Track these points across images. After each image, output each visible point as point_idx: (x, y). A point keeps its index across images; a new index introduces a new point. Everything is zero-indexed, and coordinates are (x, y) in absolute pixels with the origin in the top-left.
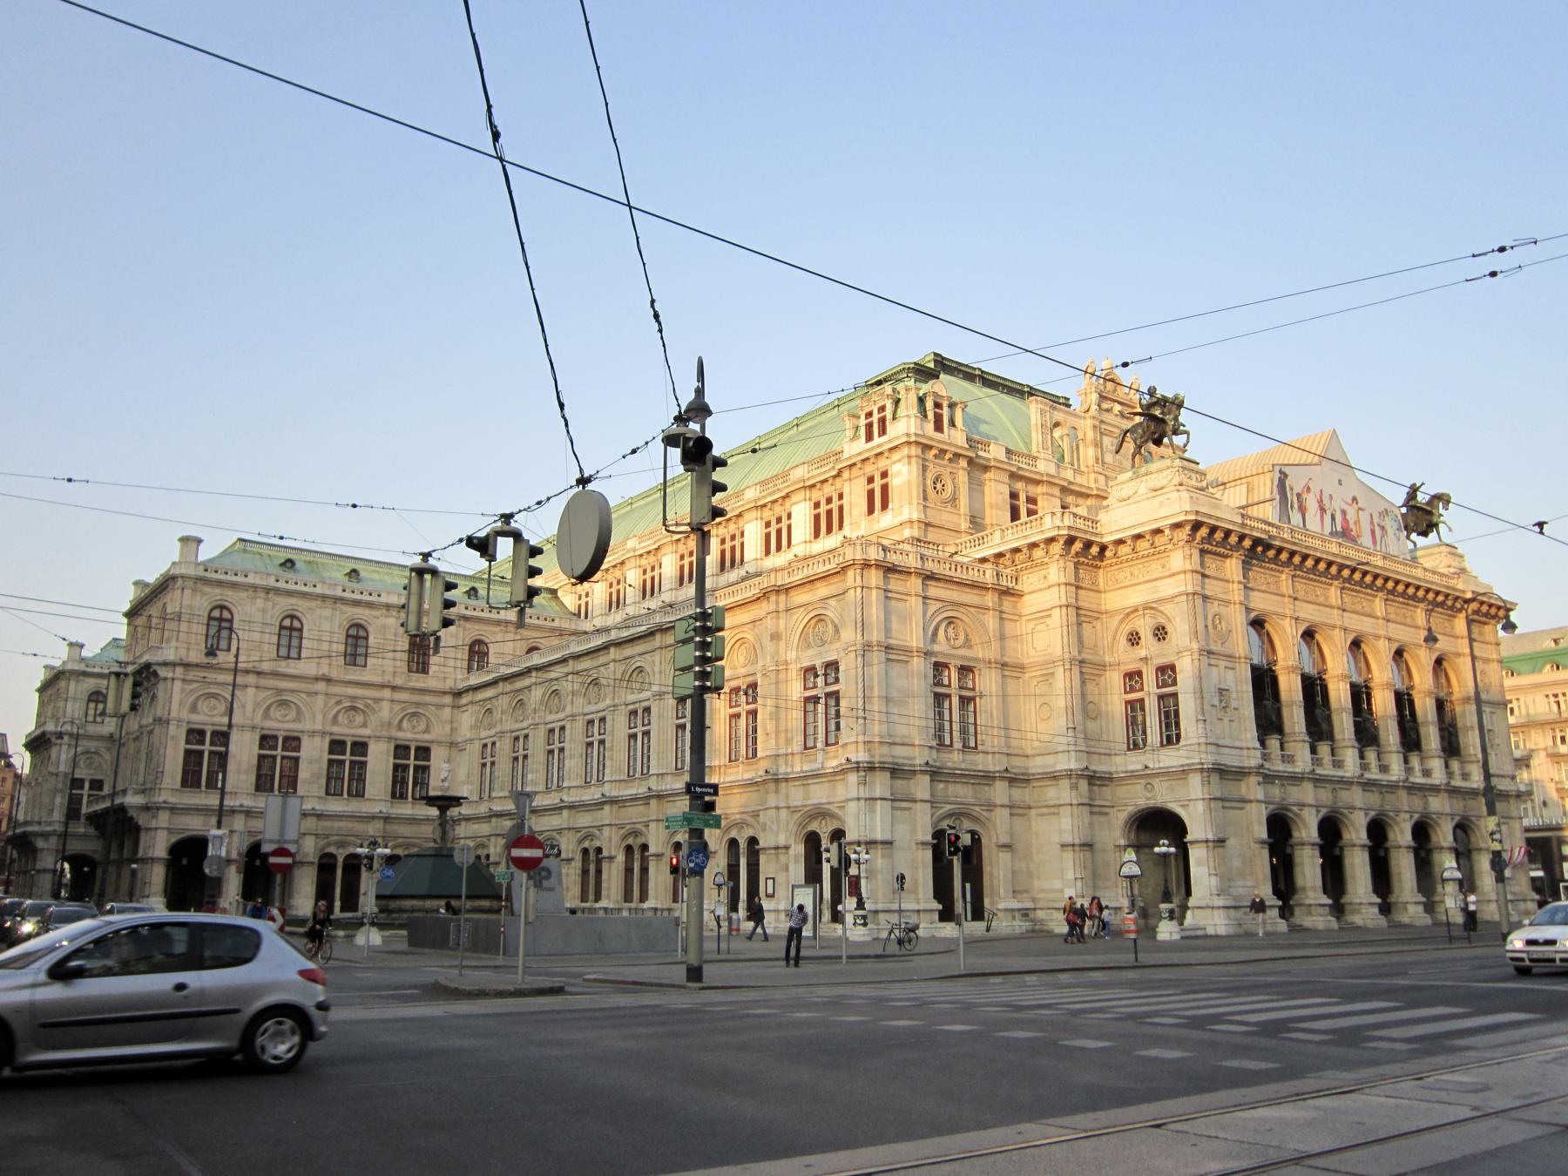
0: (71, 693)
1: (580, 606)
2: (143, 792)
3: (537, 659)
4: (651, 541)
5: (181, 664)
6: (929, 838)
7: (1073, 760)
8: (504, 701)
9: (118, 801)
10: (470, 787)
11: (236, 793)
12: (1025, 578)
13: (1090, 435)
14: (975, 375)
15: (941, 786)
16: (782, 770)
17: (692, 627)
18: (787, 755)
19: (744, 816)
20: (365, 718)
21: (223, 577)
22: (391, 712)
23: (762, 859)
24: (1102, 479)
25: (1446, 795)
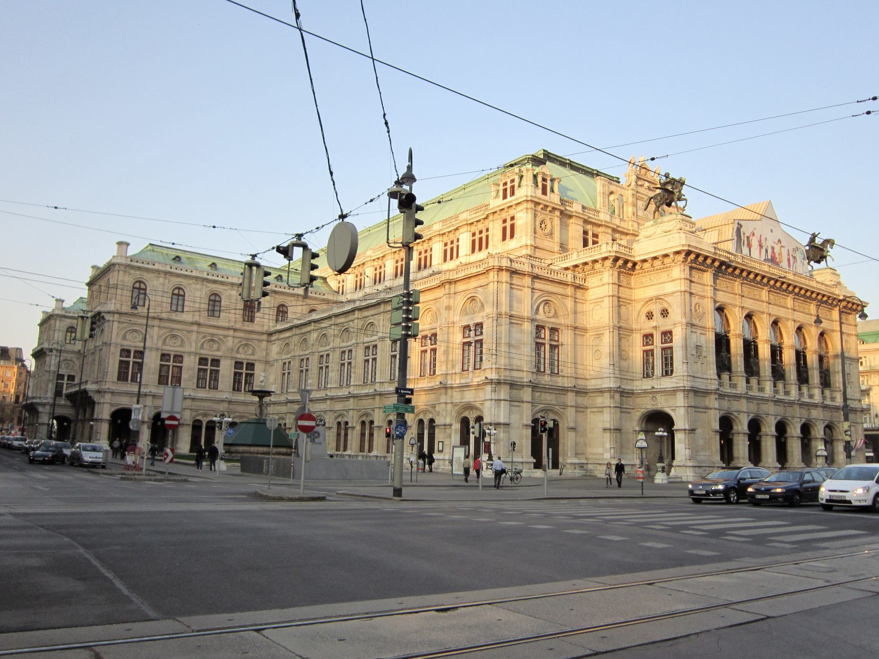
0: (57, 328)
1: (339, 287)
2: (97, 383)
3: (315, 316)
4: (380, 252)
5: (118, 313)
6: (530, 422)
7: (612, 382)
8: (296, 339)
9: (83, 387)
10: (276, 386)
11: (147, 385)
12: (590, 279)
13: (630, 199)
14: (566, 163)
15: (538, 394)
16: (449, 382)
17: (401, 301)
18: (452, 374)
19: (427, 407)
20: (219, 347)
21: (141, 265)
22: (233, 342)
23: (437, 431)
24: (636, 225)
25: (821, 409)
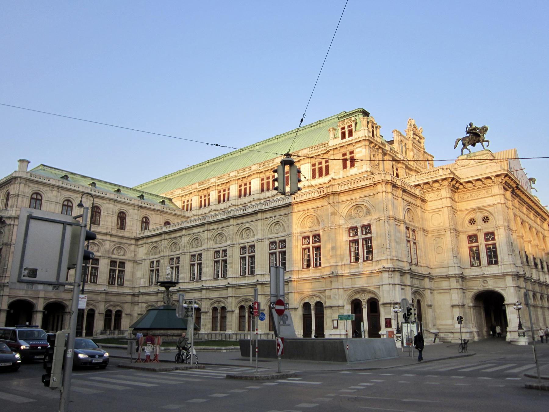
1: (184, 206)
4: (225, 179)
7: (457, 270)
8: (165, 243)
10: (144, 280)
18: (342, 265)
19: (314, 293)
20: (98, 249)
21: (39, 180)
22: (110, 245)
